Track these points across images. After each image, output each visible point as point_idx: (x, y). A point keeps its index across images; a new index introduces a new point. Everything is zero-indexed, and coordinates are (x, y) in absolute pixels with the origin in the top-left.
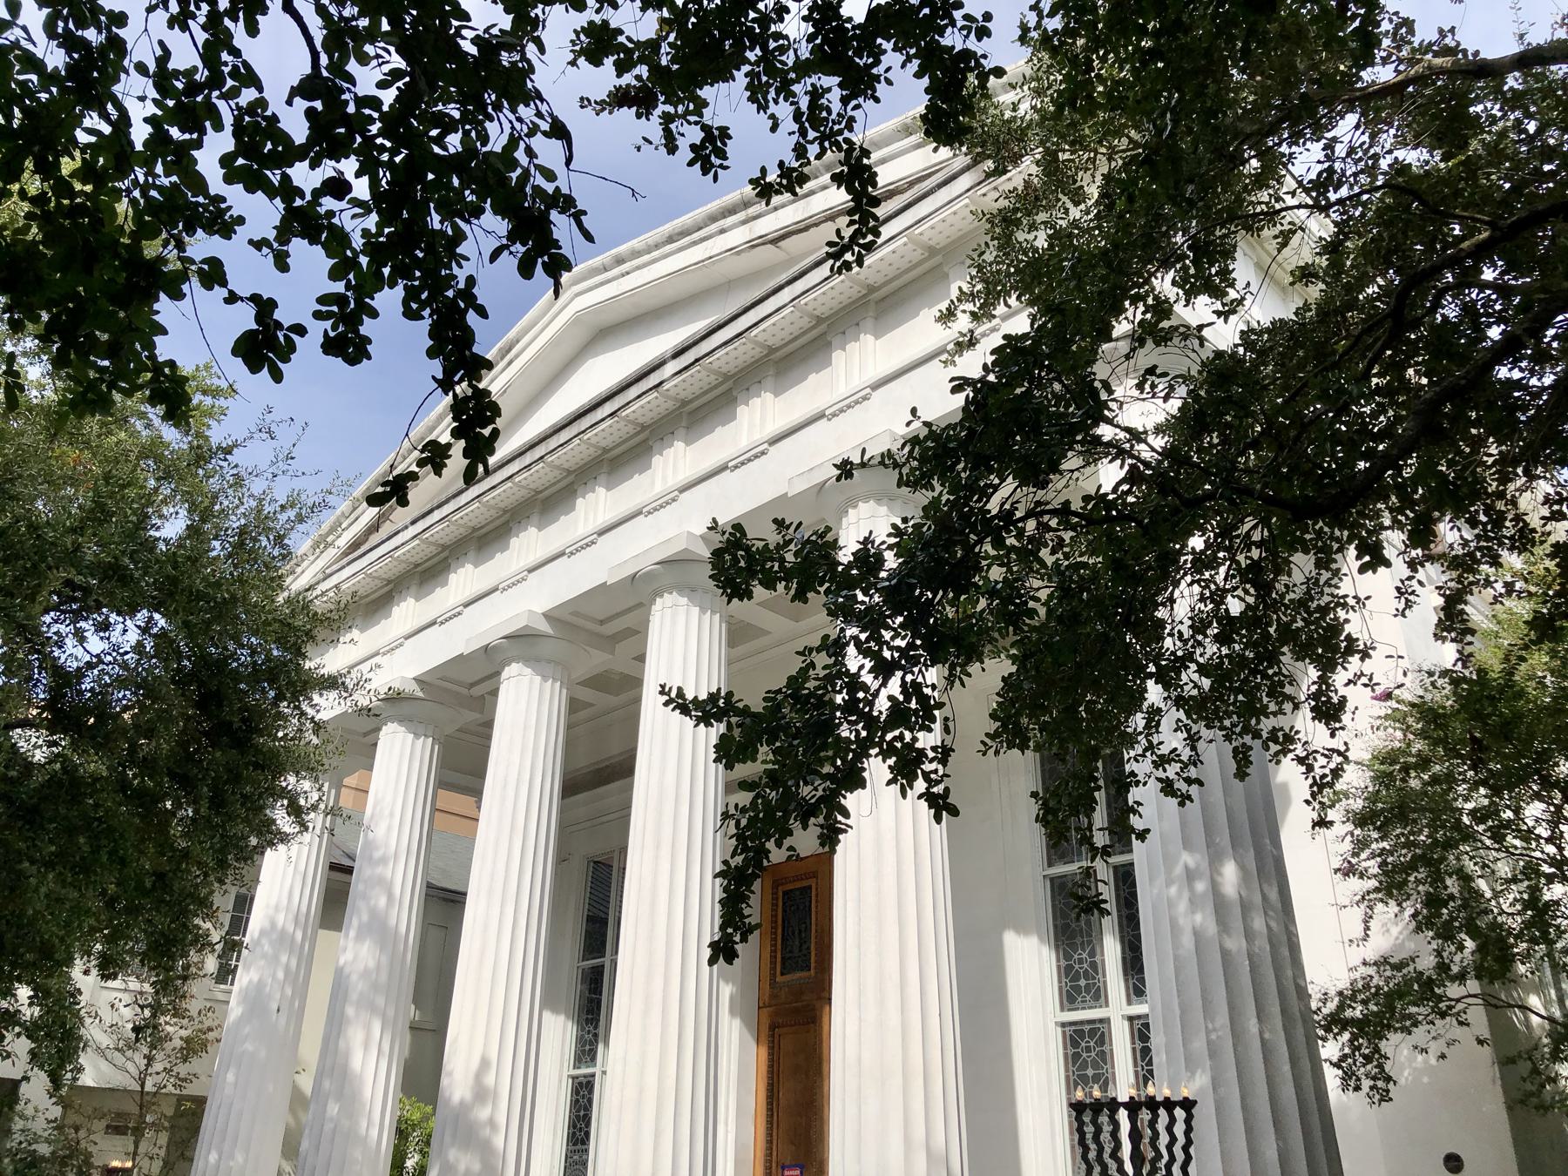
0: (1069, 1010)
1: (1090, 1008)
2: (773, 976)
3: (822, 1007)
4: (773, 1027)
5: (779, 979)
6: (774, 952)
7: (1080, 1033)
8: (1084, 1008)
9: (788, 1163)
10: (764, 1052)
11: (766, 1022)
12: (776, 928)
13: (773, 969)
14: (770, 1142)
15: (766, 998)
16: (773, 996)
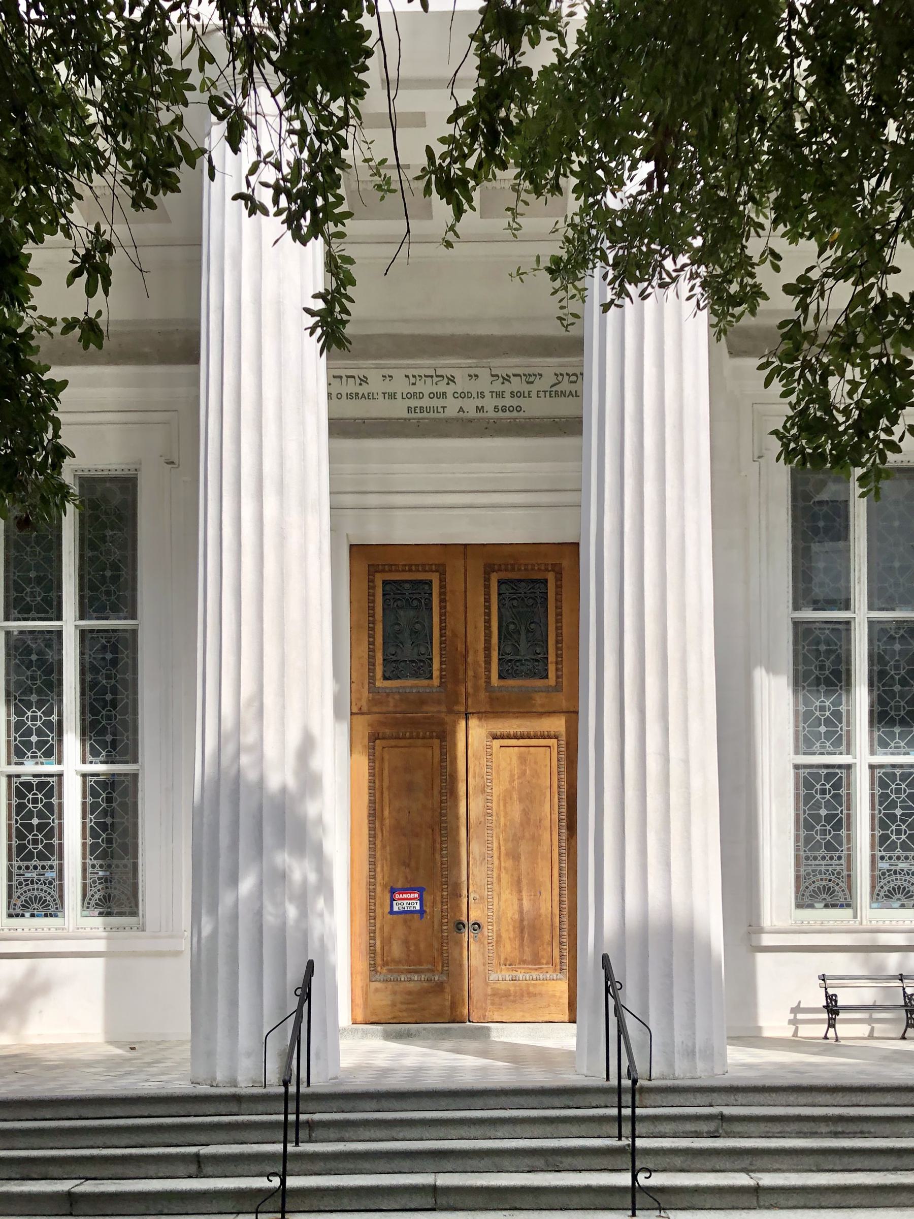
0: (805, 754)
1: (829, 754)
2: (372, 679)
3: (454, 725)
4: (374, 737)
5: (378, 684)
6: (372, 651)
7: (817, 777)
8: (822, 754)
9: (399, 885)
10: (363, 762)
11: (364, 732)
12: (374, 623)
13: (372, 670)
14: (373, 864)
15: (364, 703)
16: (373, 702)
